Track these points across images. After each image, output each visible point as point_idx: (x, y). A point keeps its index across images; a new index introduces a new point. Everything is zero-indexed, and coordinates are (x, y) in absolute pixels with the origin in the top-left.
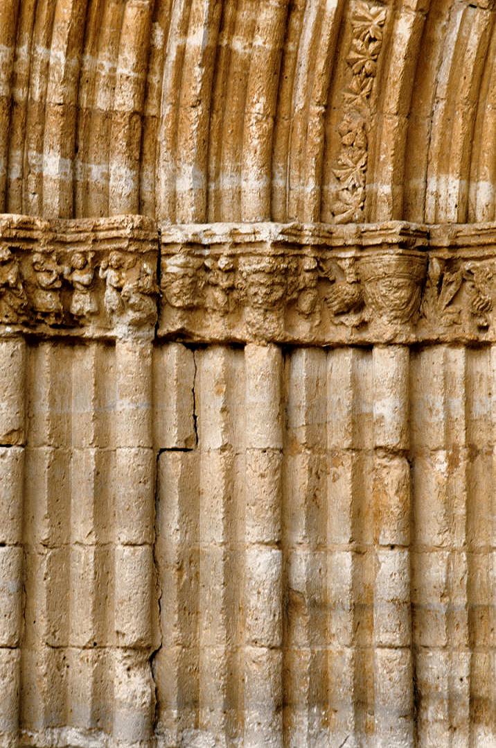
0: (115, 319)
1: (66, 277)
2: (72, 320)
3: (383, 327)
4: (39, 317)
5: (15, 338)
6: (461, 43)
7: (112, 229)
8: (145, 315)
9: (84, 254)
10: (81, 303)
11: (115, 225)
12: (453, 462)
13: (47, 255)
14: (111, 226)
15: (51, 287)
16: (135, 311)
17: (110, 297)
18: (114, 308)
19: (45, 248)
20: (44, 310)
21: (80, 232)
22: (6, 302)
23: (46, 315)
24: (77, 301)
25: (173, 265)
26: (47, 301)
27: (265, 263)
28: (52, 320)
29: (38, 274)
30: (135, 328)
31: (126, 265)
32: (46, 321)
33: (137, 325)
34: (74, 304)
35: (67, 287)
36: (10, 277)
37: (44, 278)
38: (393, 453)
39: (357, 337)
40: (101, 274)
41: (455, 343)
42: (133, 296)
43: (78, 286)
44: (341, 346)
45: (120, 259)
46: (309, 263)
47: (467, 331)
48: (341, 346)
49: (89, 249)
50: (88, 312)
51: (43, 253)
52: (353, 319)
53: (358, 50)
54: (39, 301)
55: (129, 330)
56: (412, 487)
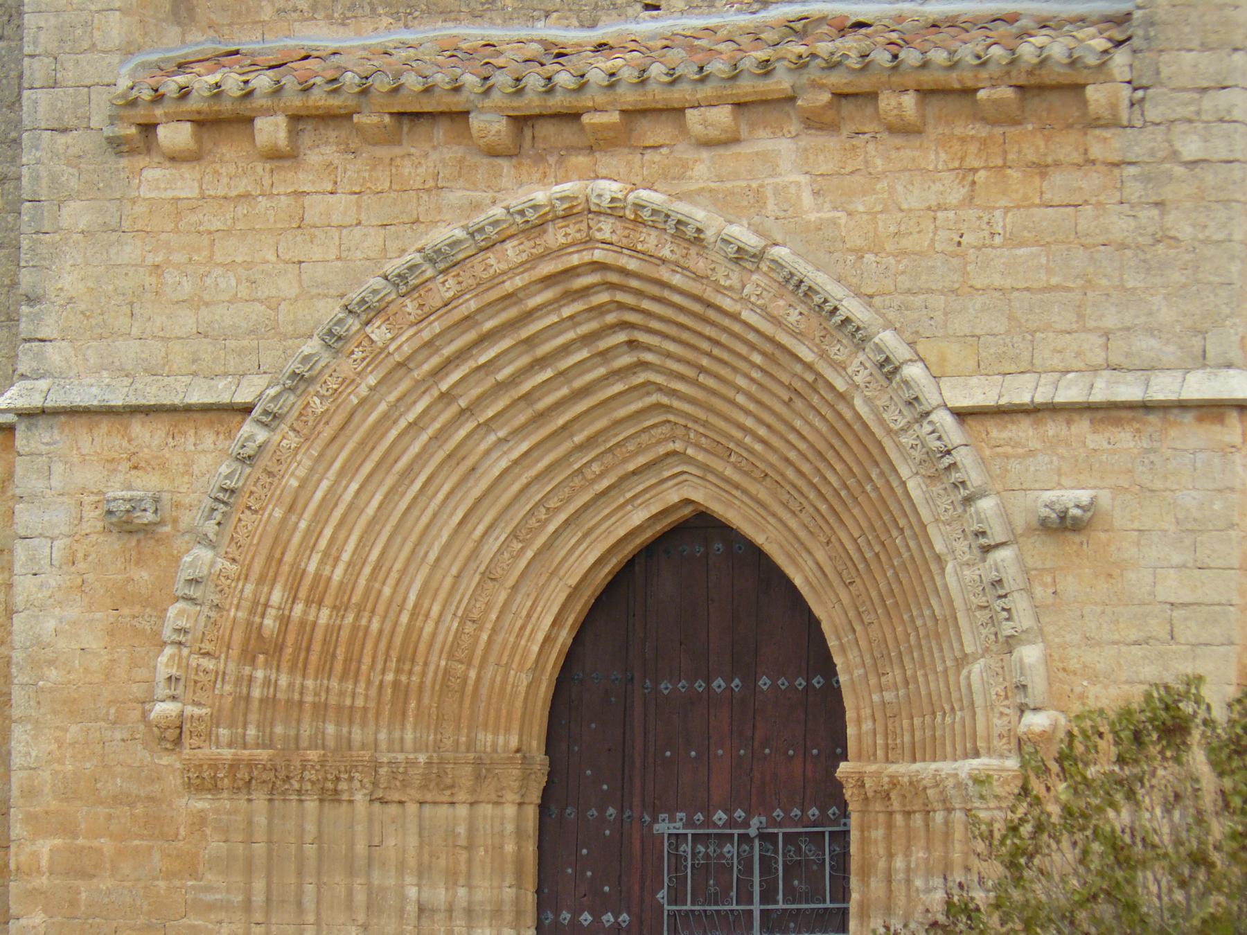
2: (336, 791)
3: (462, 796)
6: (493, 680)
12: (486, 851)
17: (356, 784)
25: (383, 771)
26: (330, 785)
27: (421, 771)
33: (365, 795)
35: (338, 779)
38: (466, 848)
39: (450, 800)
41: (488, 802)
44: (442, 803)
46: (435, 771)
47: (493, 797)
48: (442, 803)
52: (448, 792)
53: (455, 684)
56: (470, 861)
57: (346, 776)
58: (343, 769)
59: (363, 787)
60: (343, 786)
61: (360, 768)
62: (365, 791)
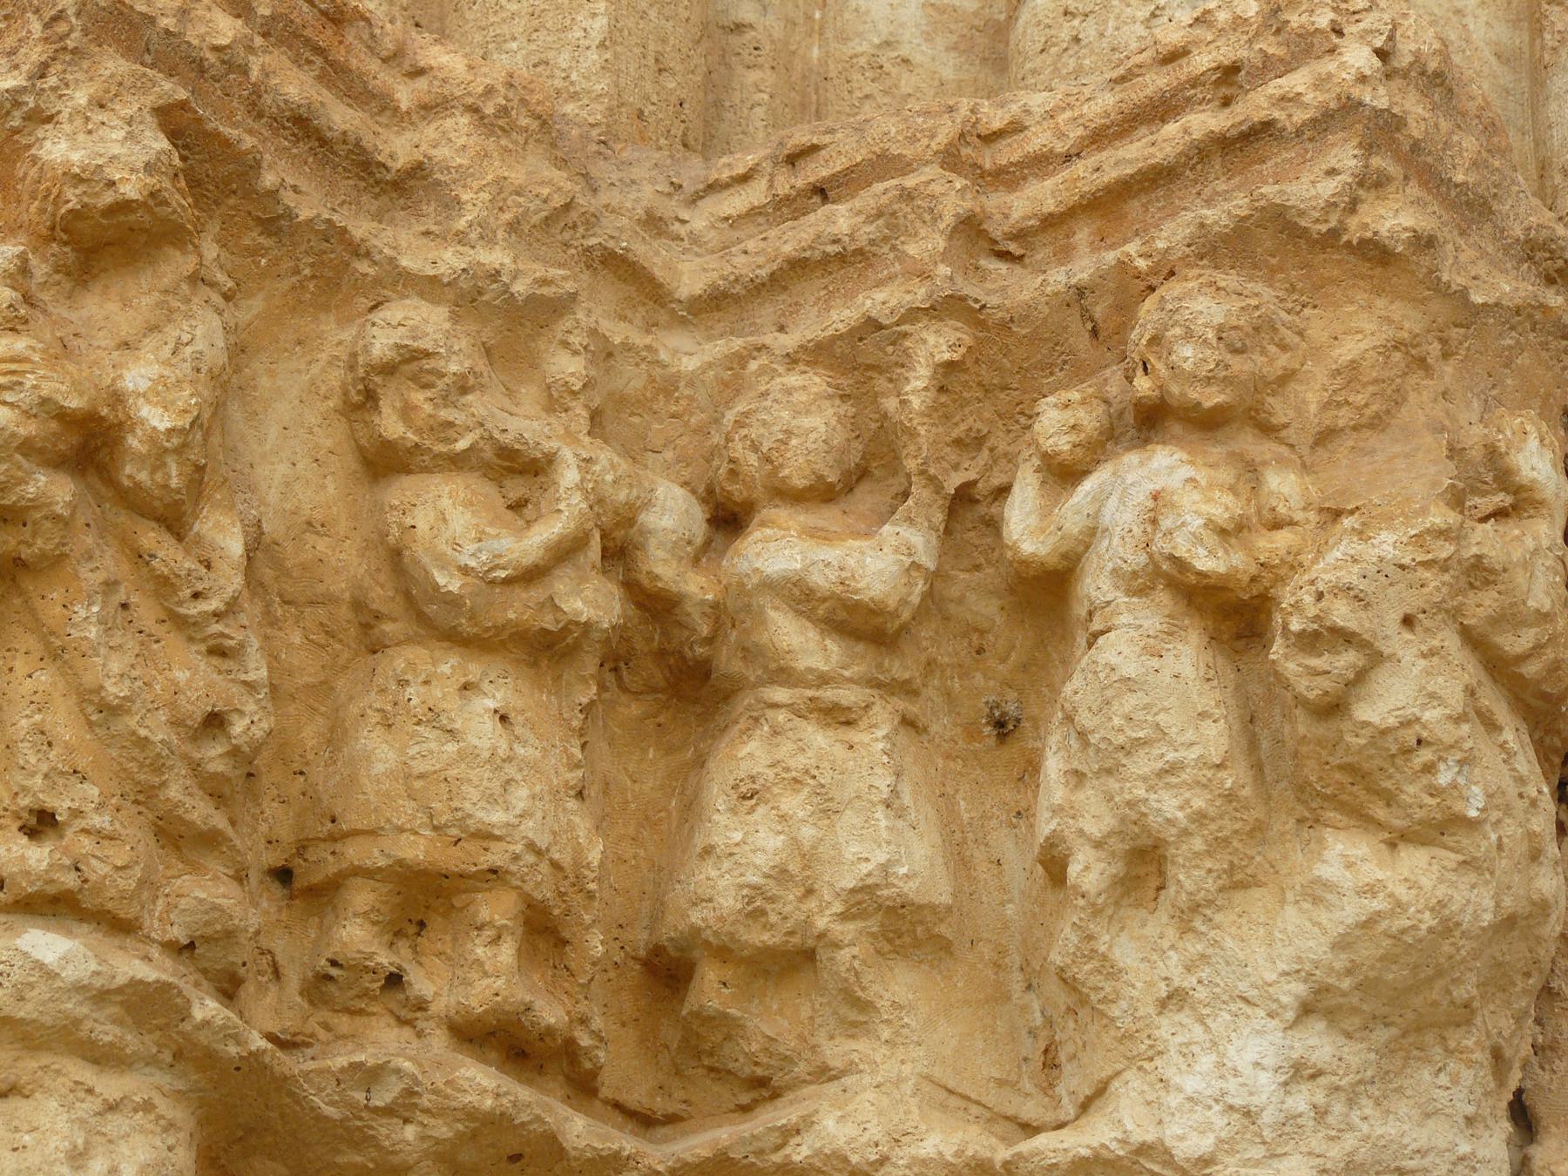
0: (1141, 953)
1: (663, 566)
4: (356, 934)
5: (104, 1058)
7: (1162, 109)
8: (1477, 903)
9: (858, 359)
10: (813, 810)
11: (1202, 61)
13: (513, 325)
14: (1157, 82)
15: (517, 609)
16: (1397, 840)
18: (1169, 806)
19: (495, 257)
20: (415, 850)
21: (821, 192)
22: (56, 654)
23: (423, 902)
24: (750, 795)
28: (485, 970)
29: (400, 490)
30: (1356, 1054)
31: (1309, 399)
32: (421, 983)
34: (724, 826)
35: (670, 675)
36: (137, 376)
37: (460, 521)
40: (1028, 527)
42: (1404, 647)
43: (791, 635)
45: (1264, 328)
49: (919, 294)
50: (864, 901)
51: (468, 297)
54: (379, 753)
55: (1300, 1072)
57: (879, 558)
58: (800, 420)
59: (1313, 766)
60: (813, 810)
61: (1196, 323)
62: (1358, 876)
